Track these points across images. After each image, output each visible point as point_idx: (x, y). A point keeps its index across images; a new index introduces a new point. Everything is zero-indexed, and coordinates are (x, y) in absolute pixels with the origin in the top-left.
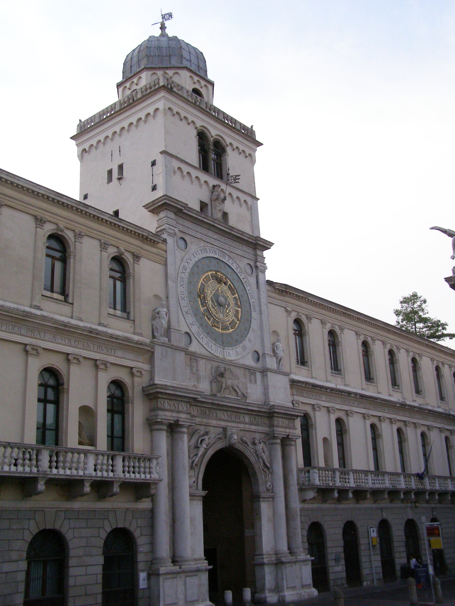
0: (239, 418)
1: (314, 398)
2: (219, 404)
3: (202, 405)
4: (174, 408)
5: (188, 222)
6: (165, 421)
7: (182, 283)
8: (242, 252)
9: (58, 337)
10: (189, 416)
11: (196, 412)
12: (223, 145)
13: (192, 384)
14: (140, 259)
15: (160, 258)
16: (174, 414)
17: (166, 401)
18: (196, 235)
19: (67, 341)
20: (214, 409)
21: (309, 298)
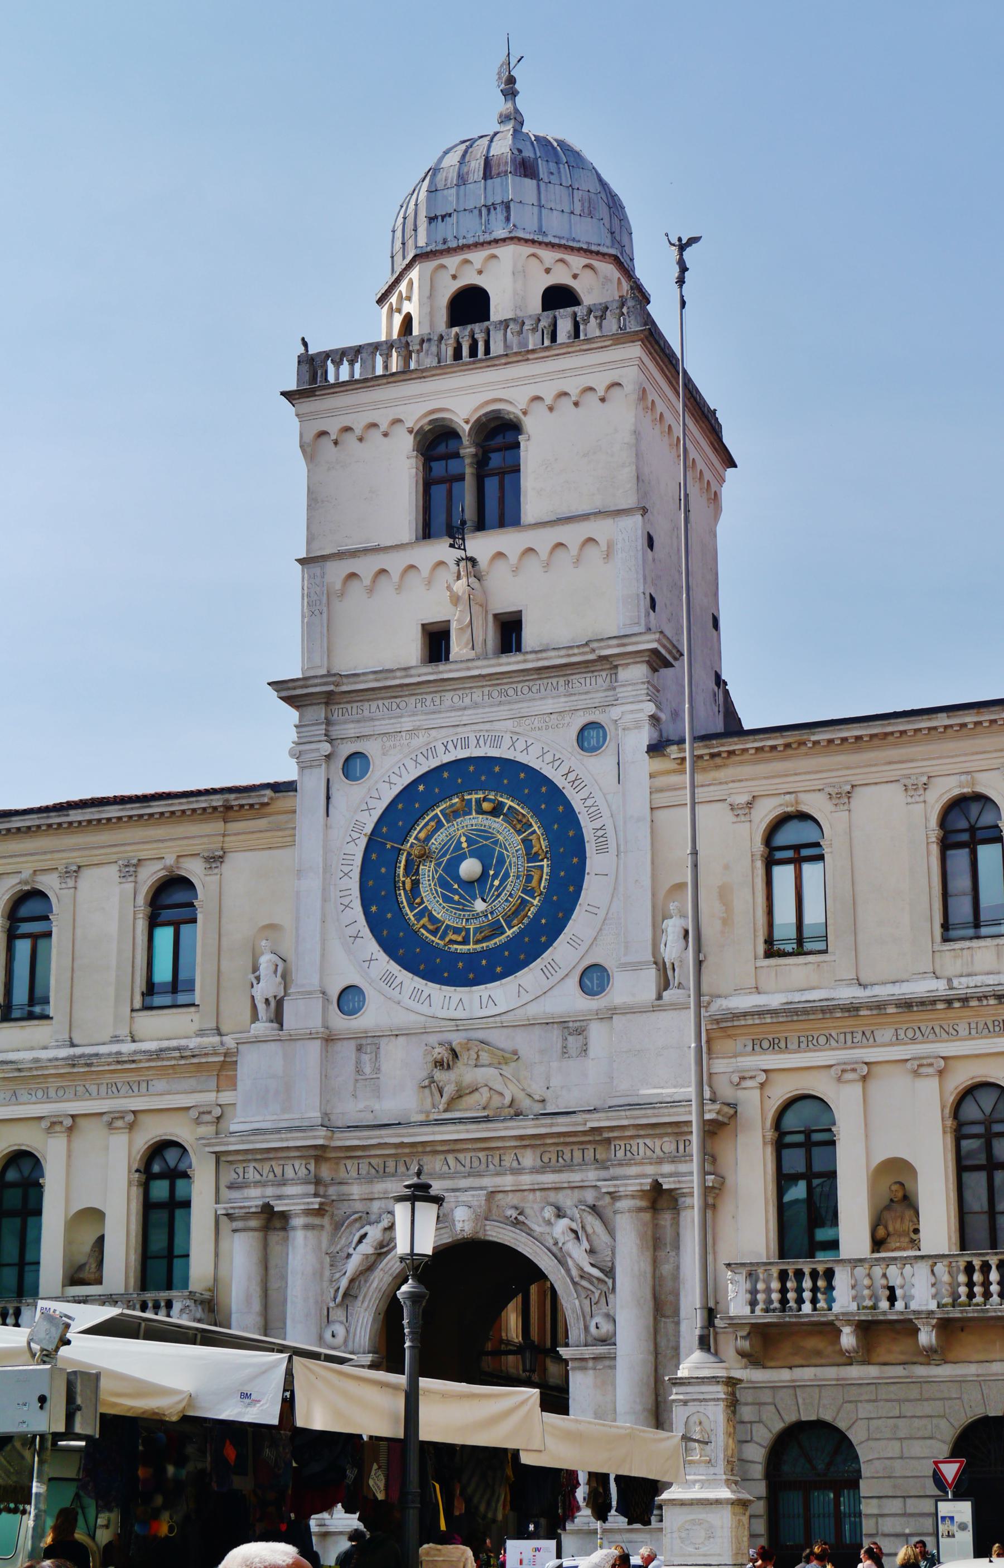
0: (500, 1160)
1: (833, 1043)
2: (403, 1143)
3: (368, 1153)
4: (271, 1175)
5: (374, 705)
6: (237, 1211)
7: (346, 869)
8: (563, 699)
9: (22, 1092)
10: (311, 1189)
11: (354, 1174)
12: (512, 416)
13: (361, 1106)
14: (222, 862)
15: (280, 833)
16: (270, 1191)
17: (252, 1164)
18: (399, 725)
19: (40, 1094)
20: (411, 1155)
21: (814, 738)
